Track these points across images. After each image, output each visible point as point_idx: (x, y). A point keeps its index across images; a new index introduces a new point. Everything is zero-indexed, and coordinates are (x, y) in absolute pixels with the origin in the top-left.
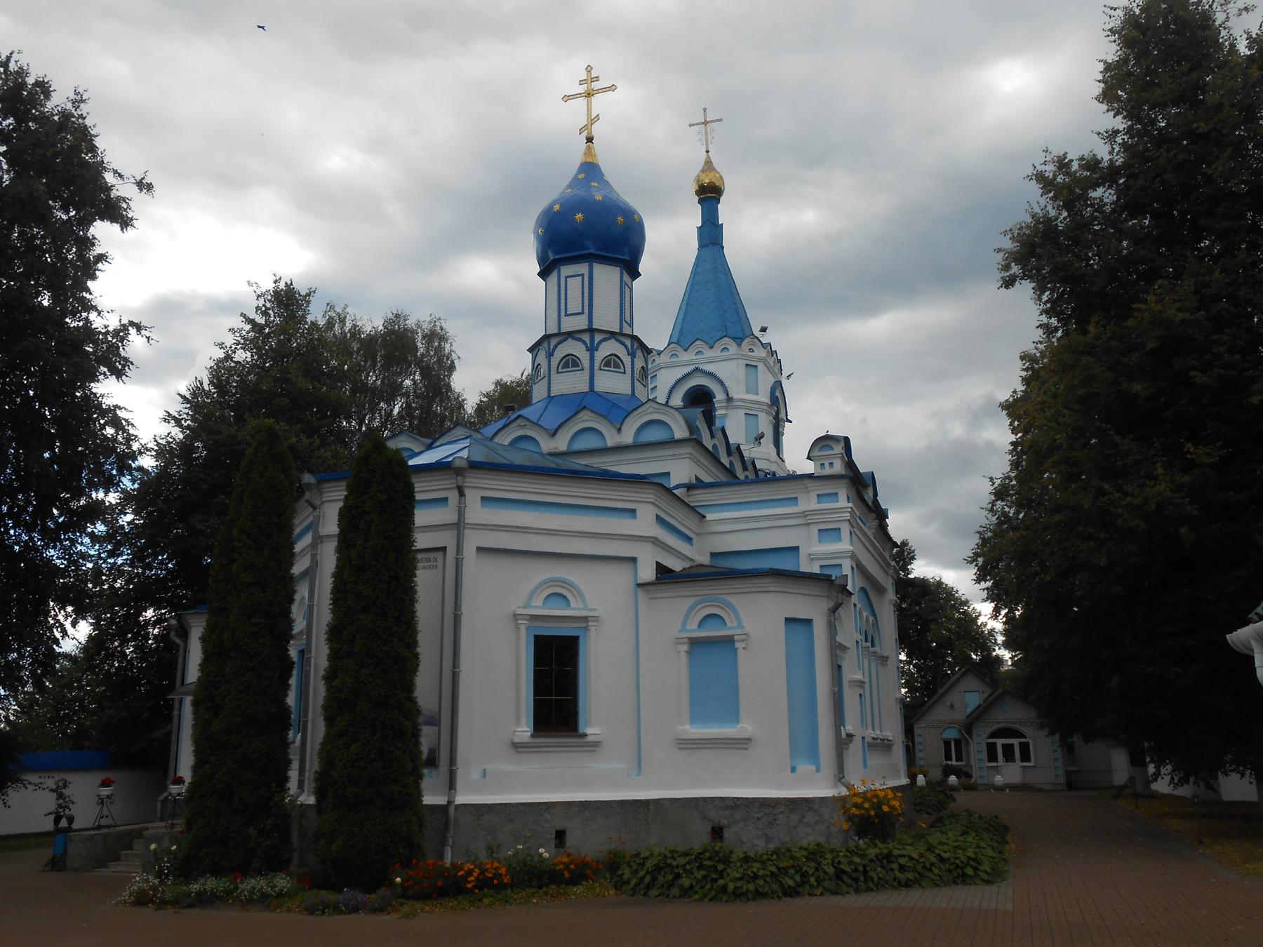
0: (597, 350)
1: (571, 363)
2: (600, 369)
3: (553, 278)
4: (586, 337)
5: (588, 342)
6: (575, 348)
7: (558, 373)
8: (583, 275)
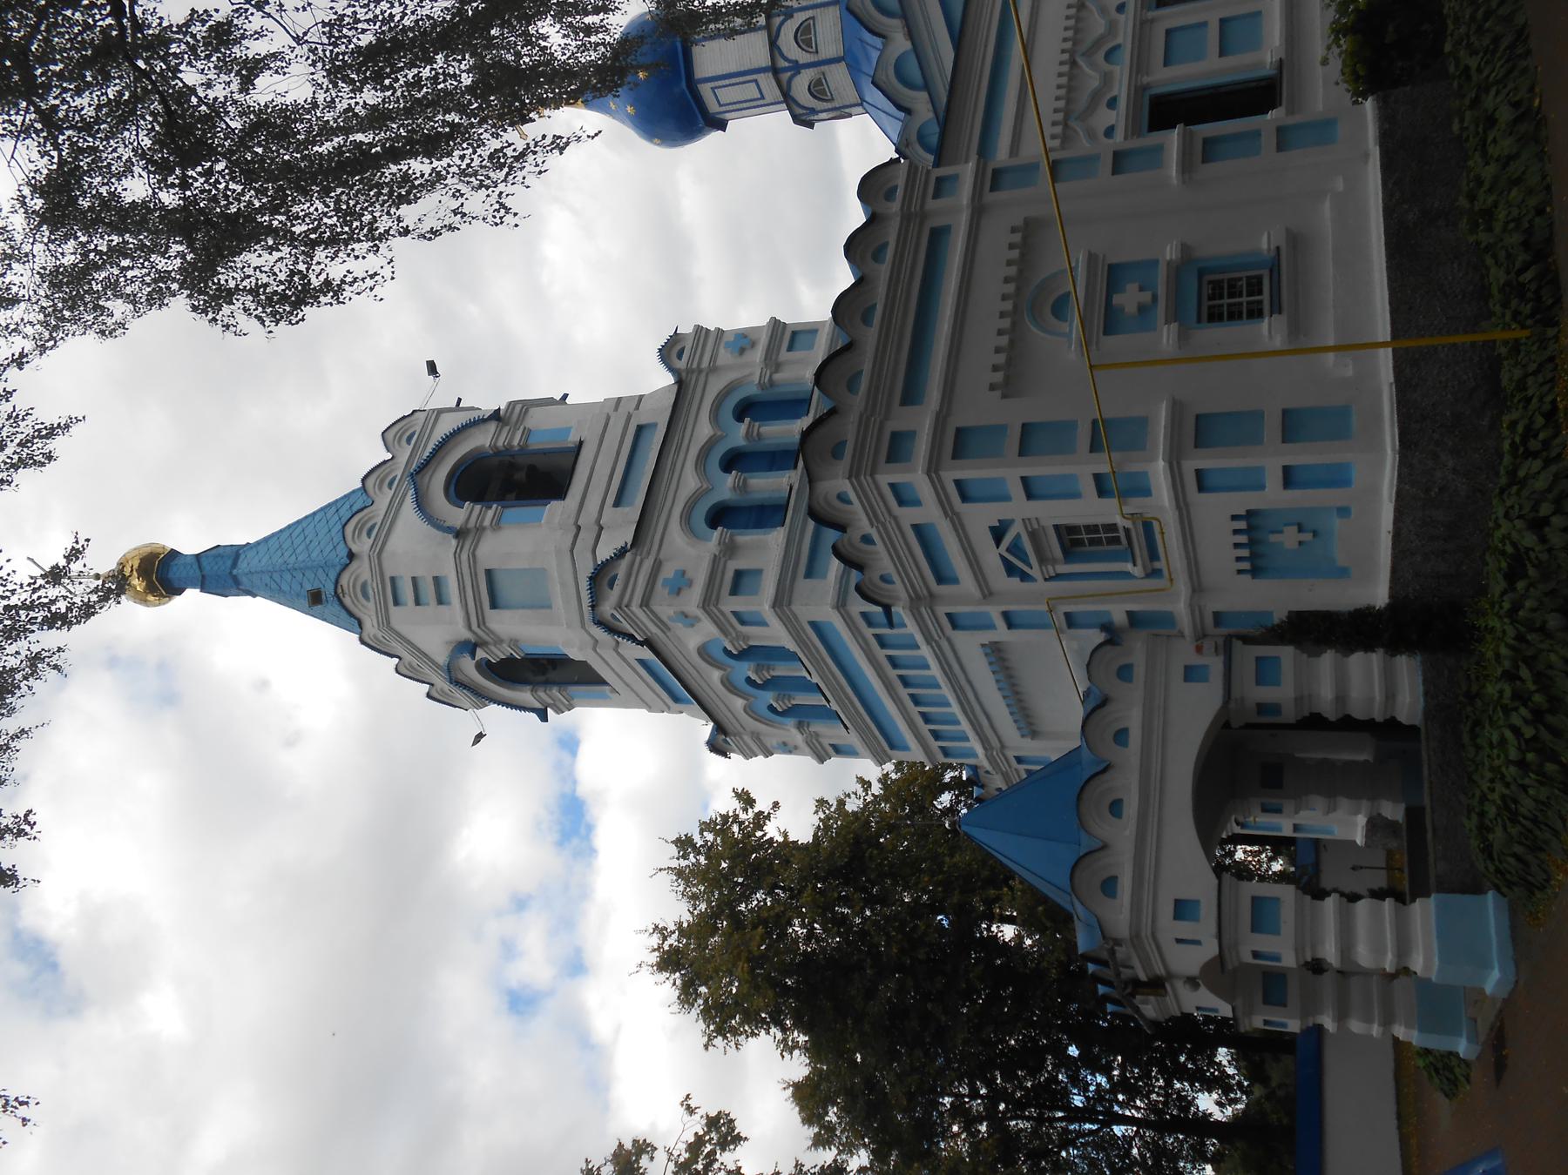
0: (797, 61)
1: (817, 89)
2: (817, 52)
3: (727, 116)
4: (785, 76)
5: (789, 74)
6: (800, 86)
7: (833, 99)
8: (713, 89)
